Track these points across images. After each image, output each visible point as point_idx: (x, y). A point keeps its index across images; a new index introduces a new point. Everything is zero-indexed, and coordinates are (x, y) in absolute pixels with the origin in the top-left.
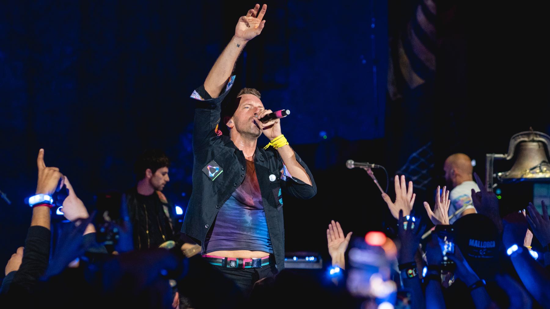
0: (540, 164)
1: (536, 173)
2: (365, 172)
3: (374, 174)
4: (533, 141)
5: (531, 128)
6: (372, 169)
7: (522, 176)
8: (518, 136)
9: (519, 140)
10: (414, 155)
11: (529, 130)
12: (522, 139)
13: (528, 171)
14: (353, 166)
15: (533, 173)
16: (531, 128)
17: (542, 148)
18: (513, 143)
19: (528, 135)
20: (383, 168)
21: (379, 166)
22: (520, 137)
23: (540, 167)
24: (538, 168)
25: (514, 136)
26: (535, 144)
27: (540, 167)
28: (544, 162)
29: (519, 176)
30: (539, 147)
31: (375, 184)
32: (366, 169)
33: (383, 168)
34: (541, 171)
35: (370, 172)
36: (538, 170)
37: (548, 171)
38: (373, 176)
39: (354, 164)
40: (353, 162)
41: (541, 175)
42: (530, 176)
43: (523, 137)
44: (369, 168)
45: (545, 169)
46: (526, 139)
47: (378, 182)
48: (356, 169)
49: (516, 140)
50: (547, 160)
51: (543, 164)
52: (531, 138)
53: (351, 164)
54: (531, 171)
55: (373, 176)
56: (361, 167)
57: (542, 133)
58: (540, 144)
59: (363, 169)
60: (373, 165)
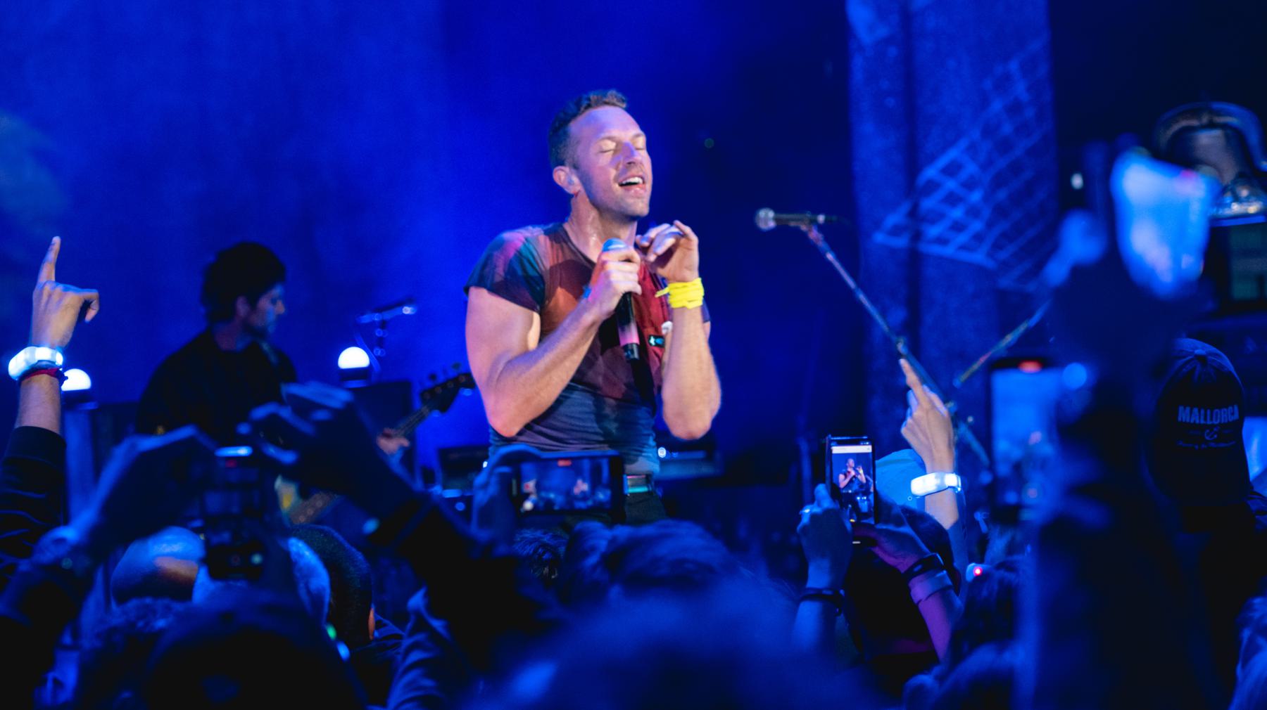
0: (1235, 182)
2: (804, 236)
3: (826, 239)
4: (1211, 126)
6: (821, 228)
9: (1176, 127)
12: (1184, 123)
14: (772, 224)
19: (1195, 113)
26: (1217, 133)
30: (1227, 137)
31: (829, 264)
32: (804, 228)
34: (1237, 199)
35: (814, 235)
38: (822, 244)
39: (776, 219)
40: (771, 214)
41: (1236, 208)
44: (812, 225)
45: (1244, 193)
46: (1194, 123)
47: (838, 257)
48: (781, 228)
52: (1205, 120)
53: (767, 218)
55: (822, 244)
56: (792, 224)
58: (1229, 132)
59: (797, 230)
60: (821, 218)
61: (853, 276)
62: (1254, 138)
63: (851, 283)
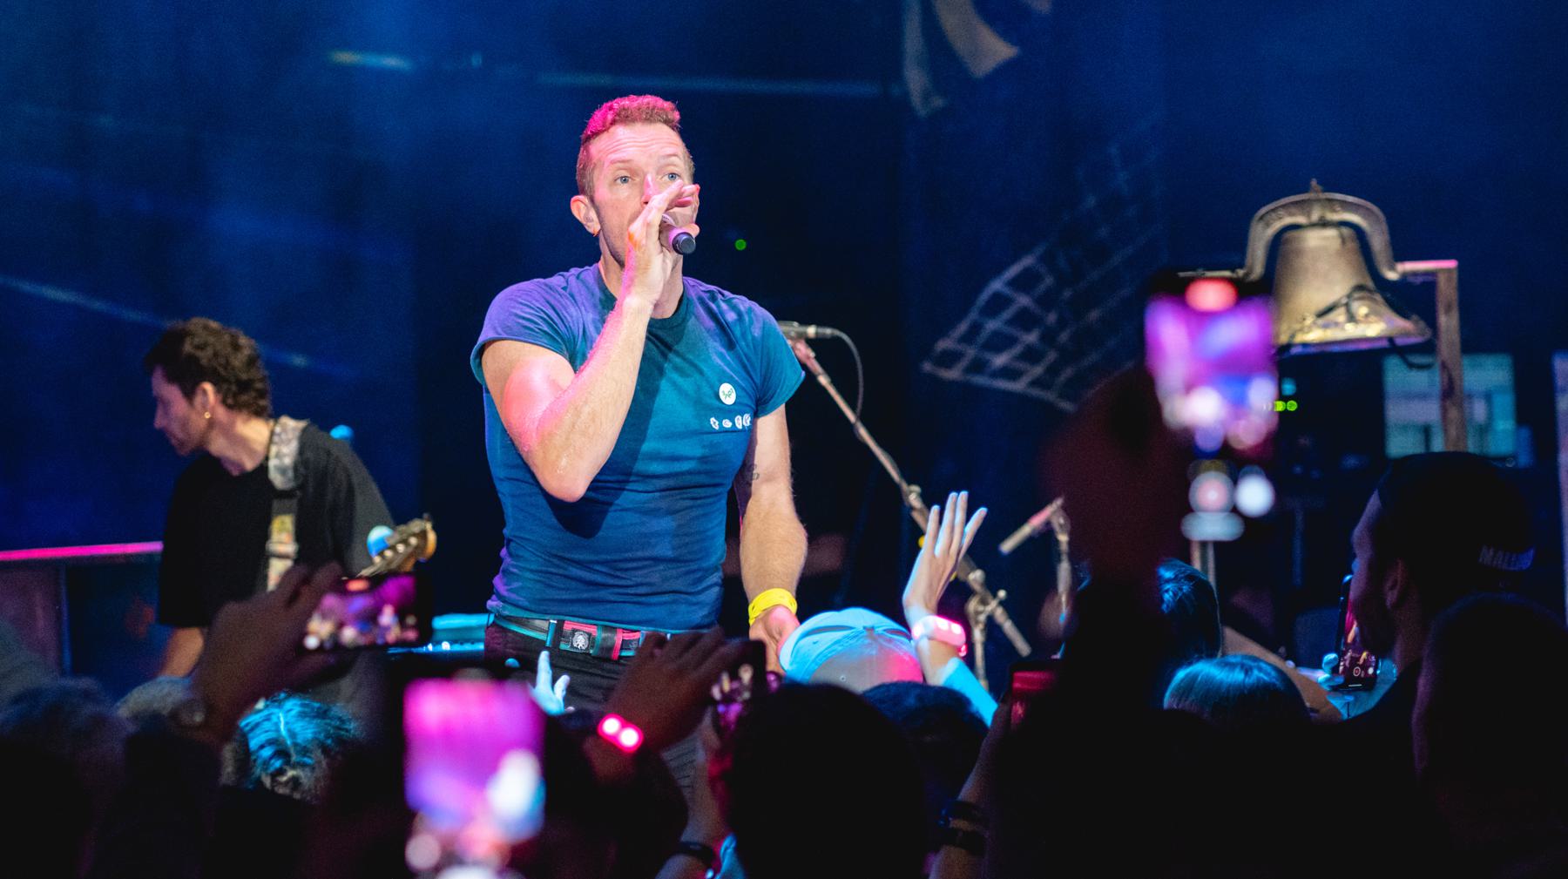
0: (1349, 296)
1: (1336, 324)
4: (1323, 224)
5: (1314, 183)
6: (811, 343)
7: (1293, 336)
8: (1273, 210)
9: (1277, 225)
10: (997, 285)
11: (1305, 189)
12: (1288, 220)
13: (1309, 322)
15: (1326, 326)
16: (1314, 183)
17: (1353, 245)
18: (1260, 236)
19: (1303, 206)
20: (845, 337)
21: (828, 331)
22: (1281, 212)
23: (1347, 305)
24: (1342, 310)
25: (1263, 210)
26: (1331, 233)
27: (1347, 305)
28: (1360, 288)
29: (1284, 339)
30: (1344, 241)
33: (845, 337)
34: (1352, 318)
36: (1339, 316)
37: (1372, 318)
41: (1351, 331)
42: (1315, 335)
43: (1291, 215)
45: (1362, 310)
46: (1301, 220)
47: (834, 382)
49: (1268, 225)
50: (1370, 284)
51: (1356, 295)
52: (1315, 217)
54: (1321, 321)
57: (1350, 199)
58: (1346, 231)
60: (811, 331)
61: (853, 407)
62: (1379, 241)
63: (851, 416)
